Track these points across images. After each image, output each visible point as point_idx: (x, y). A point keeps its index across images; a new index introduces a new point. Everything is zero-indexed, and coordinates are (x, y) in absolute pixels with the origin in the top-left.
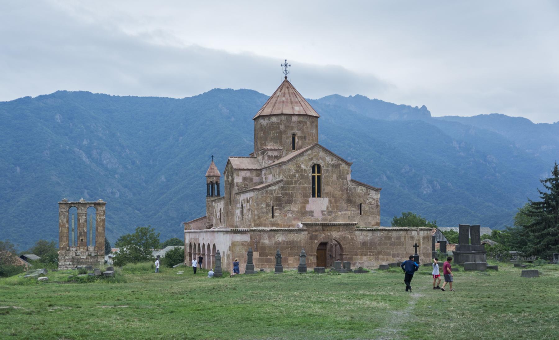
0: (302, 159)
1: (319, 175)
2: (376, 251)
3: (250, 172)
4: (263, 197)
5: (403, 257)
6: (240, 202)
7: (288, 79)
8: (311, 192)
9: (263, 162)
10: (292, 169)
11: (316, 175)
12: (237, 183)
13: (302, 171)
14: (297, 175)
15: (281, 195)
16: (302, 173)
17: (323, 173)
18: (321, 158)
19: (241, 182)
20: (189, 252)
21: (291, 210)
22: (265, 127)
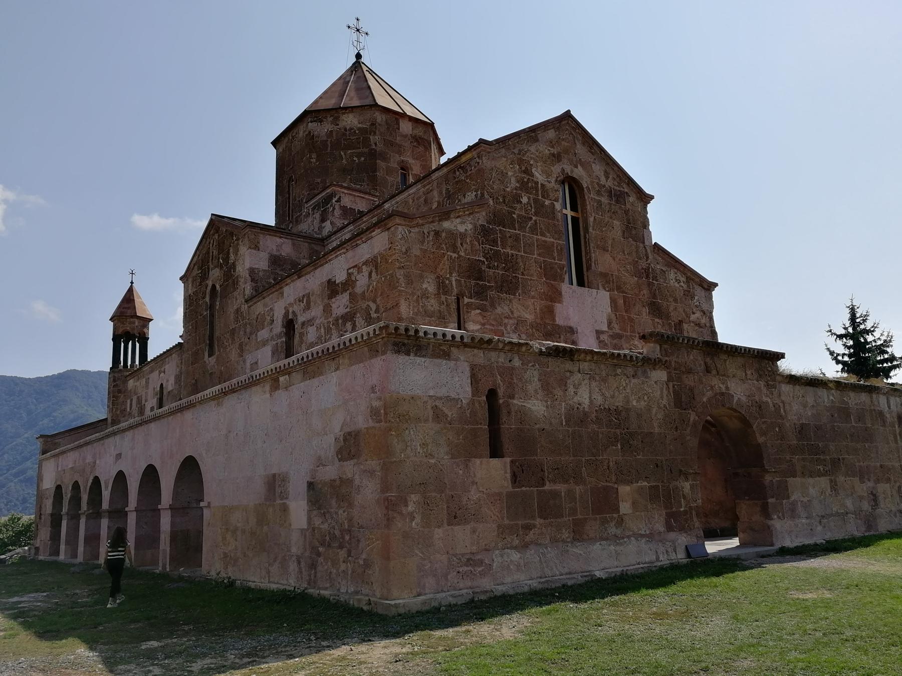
0: (533, 149)
1: (573, 214)
2: (827, 457)
3: (293, 244)
4: (427, 250)
5: (877, 481)
6: (279, 314)
7: (362, 60)
8: (564, 262)
9: (321, 228)
10: (510, 174)
11: (569, 212)
12: (252, 271)
13: (537, 191)
14: (525, 200)
15: (482, 259)
16: (537, 195)
17: (588, 207)
18: (582, 165)
19: (267, 269)
20: (52, 515)
21: (515, 315)
22: (324, 143)
